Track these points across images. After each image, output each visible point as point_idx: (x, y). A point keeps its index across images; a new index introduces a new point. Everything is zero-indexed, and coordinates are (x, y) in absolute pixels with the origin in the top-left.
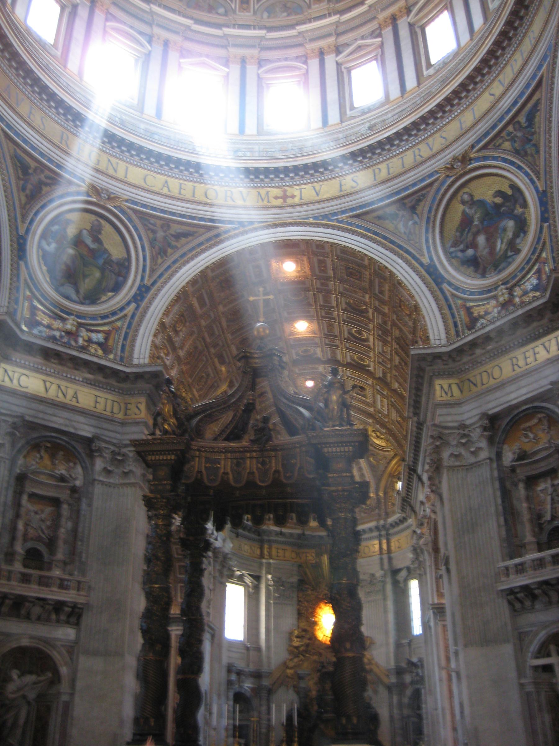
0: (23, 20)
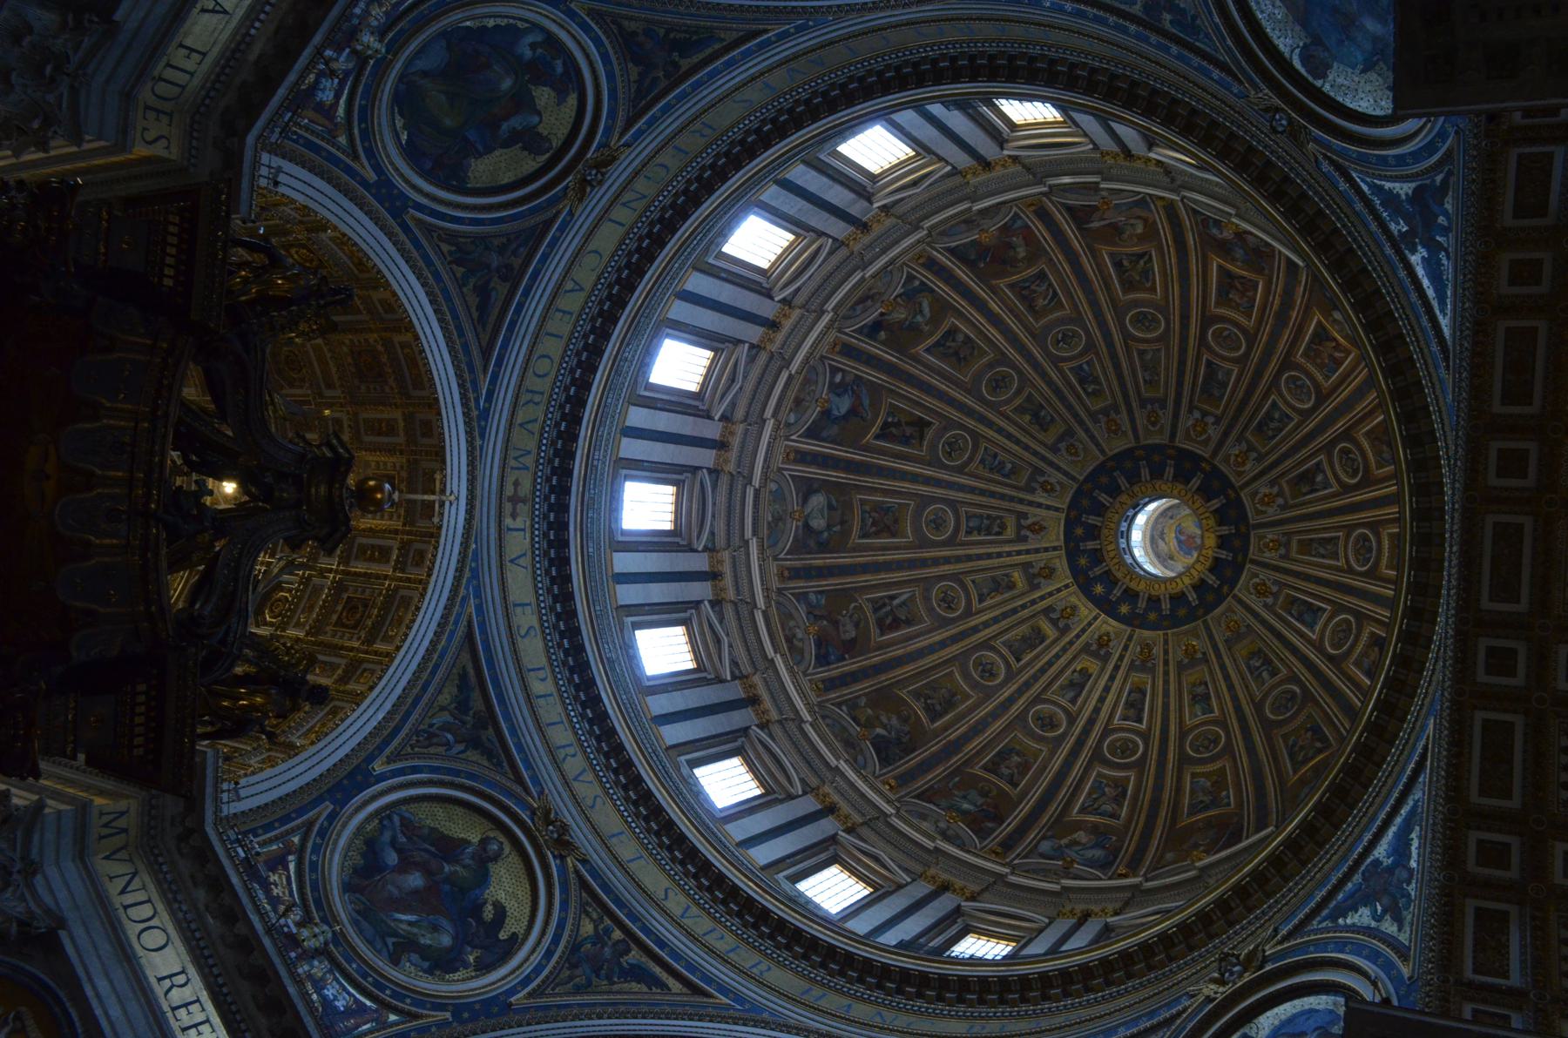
0: (896, 117)
